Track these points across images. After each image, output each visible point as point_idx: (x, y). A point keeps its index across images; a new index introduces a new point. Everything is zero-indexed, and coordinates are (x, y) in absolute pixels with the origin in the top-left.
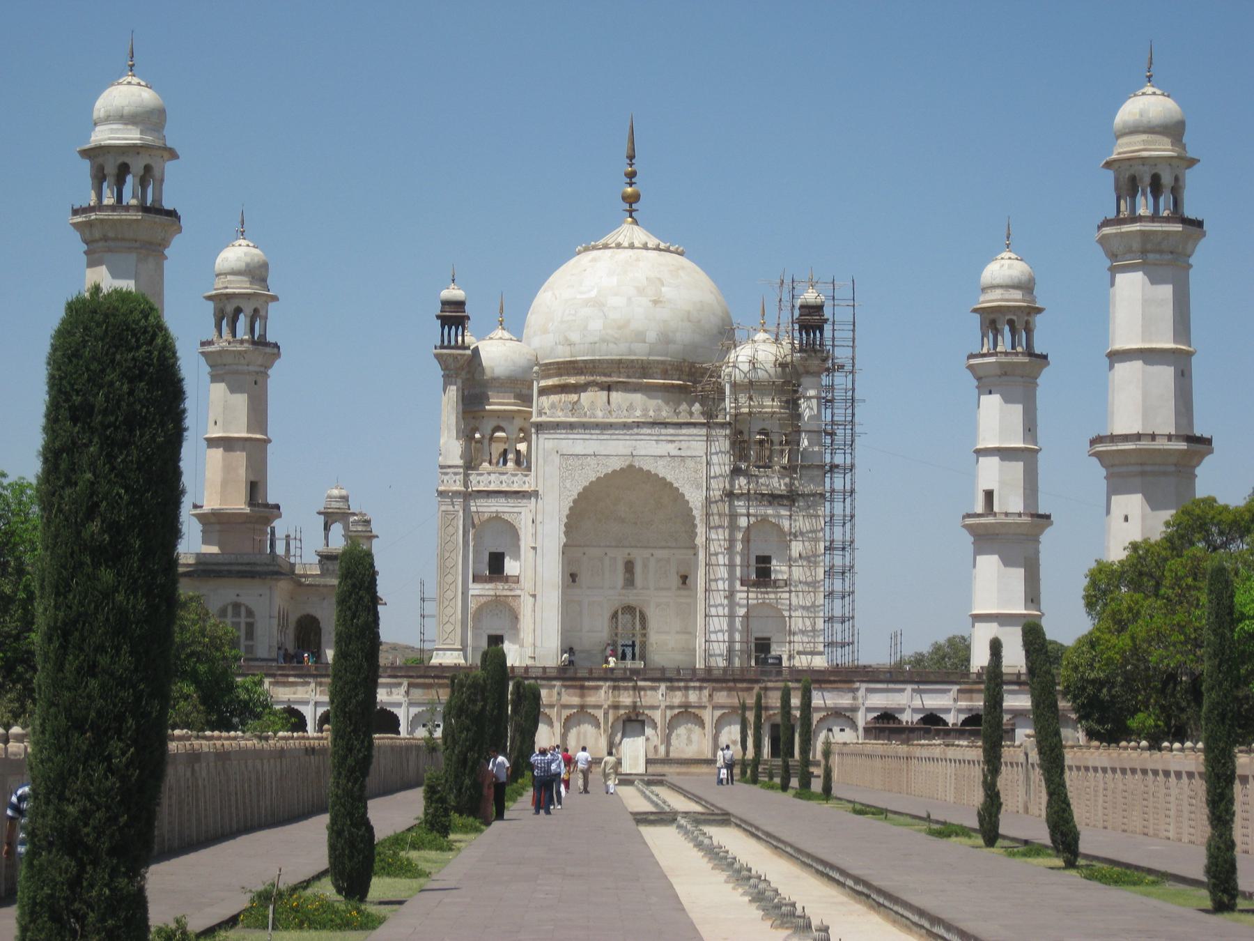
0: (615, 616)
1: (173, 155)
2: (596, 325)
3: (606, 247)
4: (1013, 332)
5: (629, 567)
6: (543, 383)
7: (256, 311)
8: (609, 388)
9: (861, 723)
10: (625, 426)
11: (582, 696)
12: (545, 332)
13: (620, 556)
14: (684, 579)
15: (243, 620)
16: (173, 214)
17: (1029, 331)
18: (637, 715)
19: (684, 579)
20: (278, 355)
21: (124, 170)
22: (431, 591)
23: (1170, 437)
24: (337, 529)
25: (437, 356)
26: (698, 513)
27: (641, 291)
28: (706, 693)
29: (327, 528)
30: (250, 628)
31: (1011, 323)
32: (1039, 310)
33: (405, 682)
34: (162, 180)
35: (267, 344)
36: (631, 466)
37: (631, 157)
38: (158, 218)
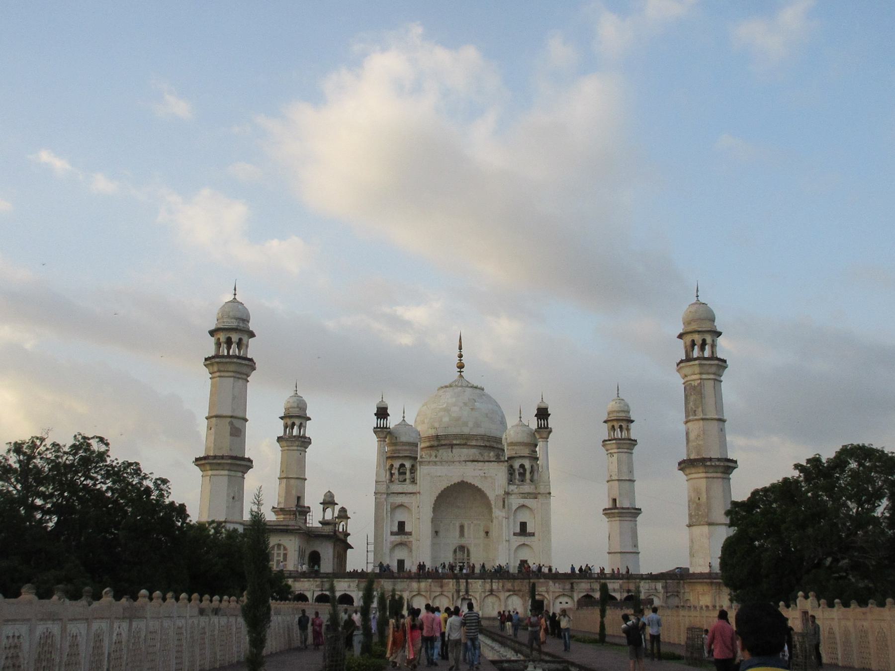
0: (455, 551)
1: (252, 335)
2: (446, 419)
3: (451, 386)
4: (621, 431)
5: (462, 527)
6: (423, 445)
7: (301, 424)
8: (452, 446)
9: (576, 599)
10: (460, 462)
11: (441, 587)
12: (423, 423)
13: (458, 525)
14: (487, 533)
15: (282, 552)
16: (251, 360)
17: (628, 430)
18: (469, 595)
19: (487, 533)
20: (310, 443)
21: (229, 342)
22: (371, 540)
23: (719, 460)
24: (329, 511)
25: (375, 432)
26: (493, 503)
27: (465, 404)
28: (501, 584)
29: (324, 510)
30: (285, 555)
31: (621, 427)
32: (632, 421)
33: (357, 580)
34: (247, 346)
35: (305, 438)
36: (463, 481)
37: (460, 348)
38: (244, 362)
